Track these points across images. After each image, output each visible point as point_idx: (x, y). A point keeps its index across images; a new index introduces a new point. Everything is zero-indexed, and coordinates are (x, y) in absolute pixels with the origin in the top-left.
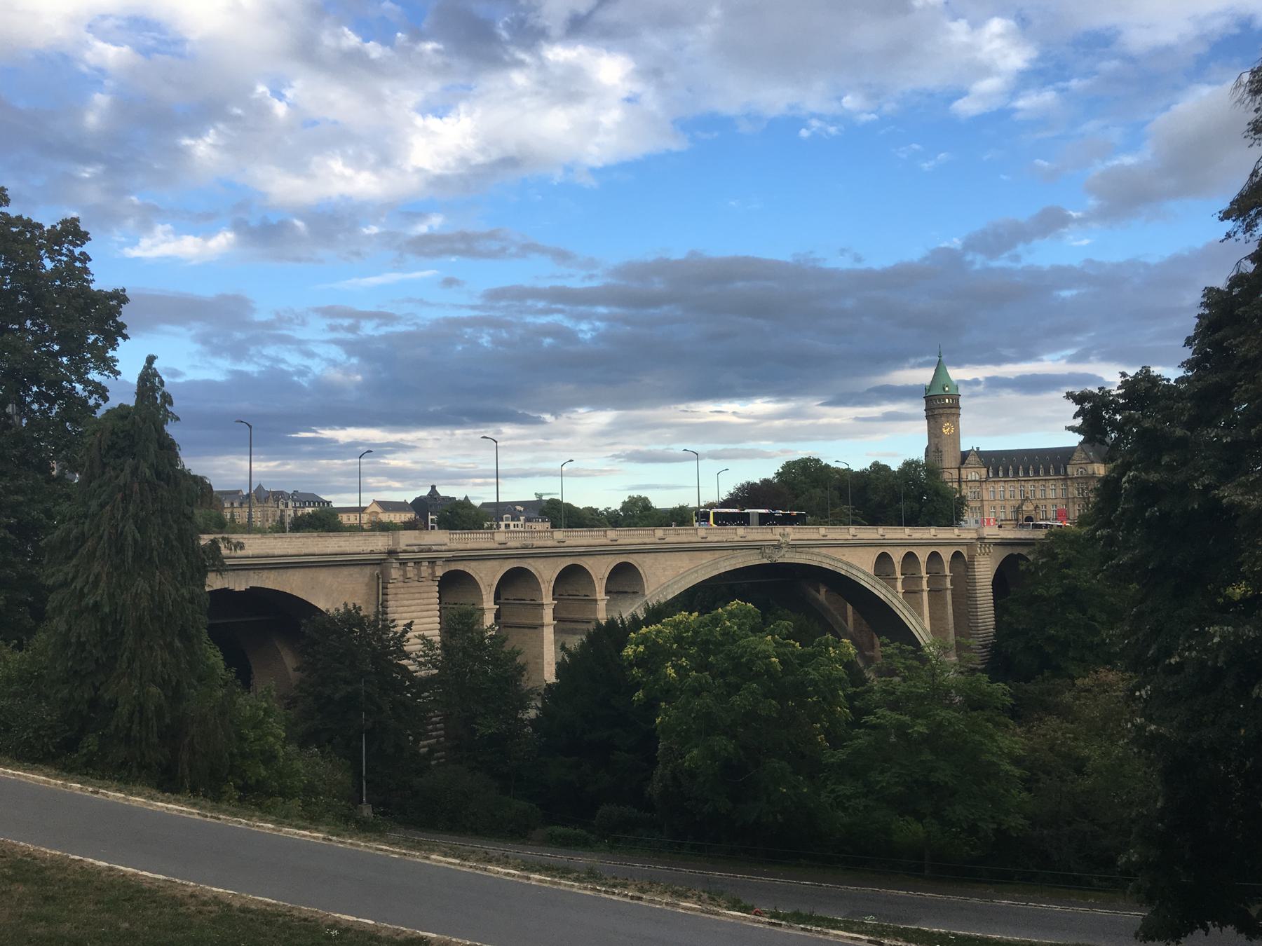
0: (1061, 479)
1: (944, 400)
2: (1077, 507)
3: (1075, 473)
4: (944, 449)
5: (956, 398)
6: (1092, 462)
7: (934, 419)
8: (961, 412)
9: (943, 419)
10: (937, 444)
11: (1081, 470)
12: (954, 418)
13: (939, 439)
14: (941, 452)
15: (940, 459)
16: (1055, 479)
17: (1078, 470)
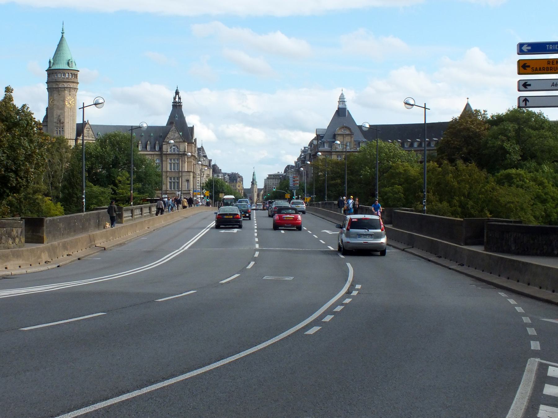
0: (156, 154)
1: (64, 74)
2: (168, 179)
3: (169, 150)
4: (66, 121)
5: (75, 74)
6: (184, 142)
7: (58, 91)
8: (79, 86)
9: (66, 92)
10: (59, 116)
11: (174, 147)
12: (73, 92)
13: (61, 111)
14: (63, 123)
15: (61, 129)
16: (151, 154)
17: (171, 148)
